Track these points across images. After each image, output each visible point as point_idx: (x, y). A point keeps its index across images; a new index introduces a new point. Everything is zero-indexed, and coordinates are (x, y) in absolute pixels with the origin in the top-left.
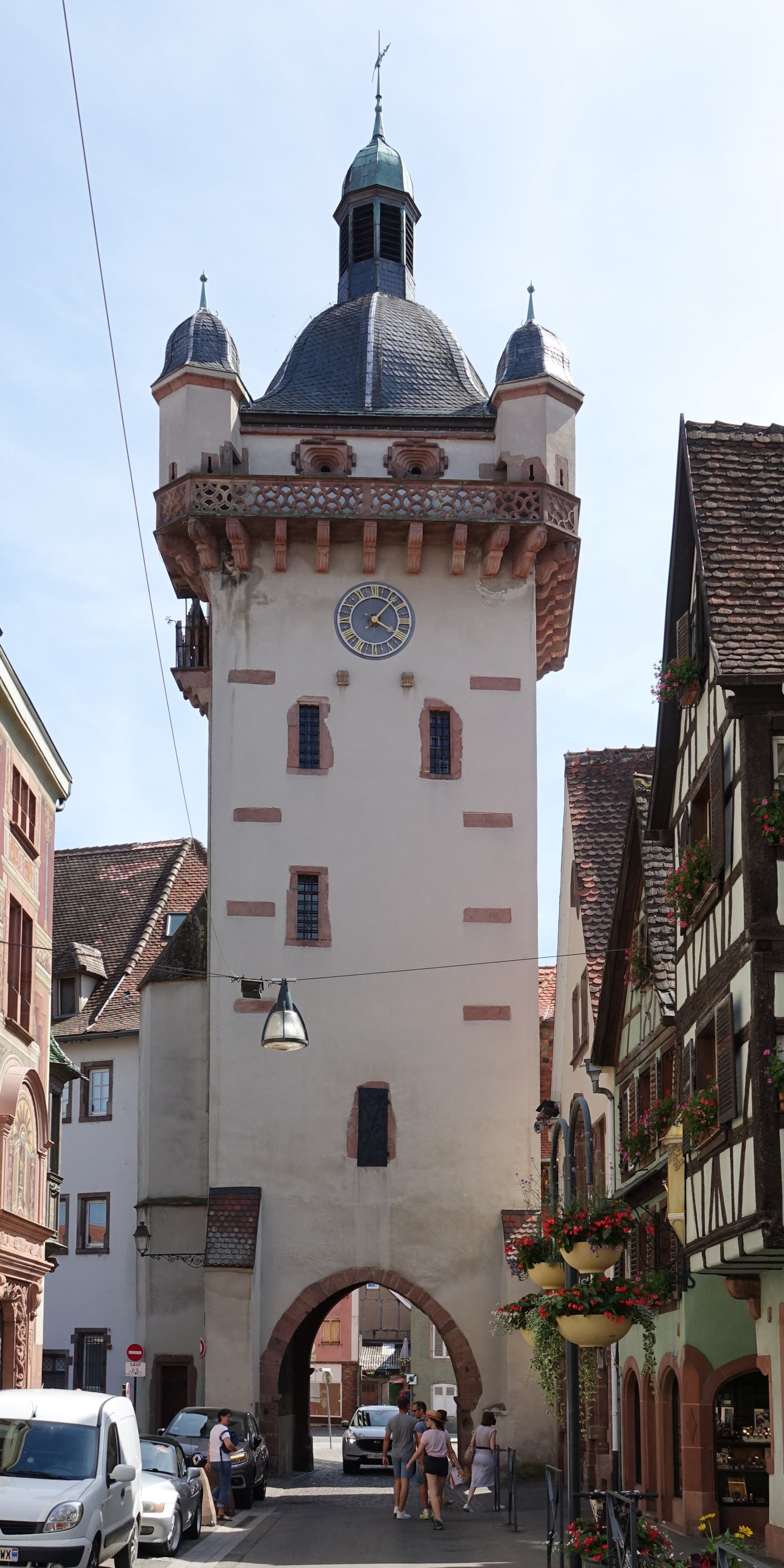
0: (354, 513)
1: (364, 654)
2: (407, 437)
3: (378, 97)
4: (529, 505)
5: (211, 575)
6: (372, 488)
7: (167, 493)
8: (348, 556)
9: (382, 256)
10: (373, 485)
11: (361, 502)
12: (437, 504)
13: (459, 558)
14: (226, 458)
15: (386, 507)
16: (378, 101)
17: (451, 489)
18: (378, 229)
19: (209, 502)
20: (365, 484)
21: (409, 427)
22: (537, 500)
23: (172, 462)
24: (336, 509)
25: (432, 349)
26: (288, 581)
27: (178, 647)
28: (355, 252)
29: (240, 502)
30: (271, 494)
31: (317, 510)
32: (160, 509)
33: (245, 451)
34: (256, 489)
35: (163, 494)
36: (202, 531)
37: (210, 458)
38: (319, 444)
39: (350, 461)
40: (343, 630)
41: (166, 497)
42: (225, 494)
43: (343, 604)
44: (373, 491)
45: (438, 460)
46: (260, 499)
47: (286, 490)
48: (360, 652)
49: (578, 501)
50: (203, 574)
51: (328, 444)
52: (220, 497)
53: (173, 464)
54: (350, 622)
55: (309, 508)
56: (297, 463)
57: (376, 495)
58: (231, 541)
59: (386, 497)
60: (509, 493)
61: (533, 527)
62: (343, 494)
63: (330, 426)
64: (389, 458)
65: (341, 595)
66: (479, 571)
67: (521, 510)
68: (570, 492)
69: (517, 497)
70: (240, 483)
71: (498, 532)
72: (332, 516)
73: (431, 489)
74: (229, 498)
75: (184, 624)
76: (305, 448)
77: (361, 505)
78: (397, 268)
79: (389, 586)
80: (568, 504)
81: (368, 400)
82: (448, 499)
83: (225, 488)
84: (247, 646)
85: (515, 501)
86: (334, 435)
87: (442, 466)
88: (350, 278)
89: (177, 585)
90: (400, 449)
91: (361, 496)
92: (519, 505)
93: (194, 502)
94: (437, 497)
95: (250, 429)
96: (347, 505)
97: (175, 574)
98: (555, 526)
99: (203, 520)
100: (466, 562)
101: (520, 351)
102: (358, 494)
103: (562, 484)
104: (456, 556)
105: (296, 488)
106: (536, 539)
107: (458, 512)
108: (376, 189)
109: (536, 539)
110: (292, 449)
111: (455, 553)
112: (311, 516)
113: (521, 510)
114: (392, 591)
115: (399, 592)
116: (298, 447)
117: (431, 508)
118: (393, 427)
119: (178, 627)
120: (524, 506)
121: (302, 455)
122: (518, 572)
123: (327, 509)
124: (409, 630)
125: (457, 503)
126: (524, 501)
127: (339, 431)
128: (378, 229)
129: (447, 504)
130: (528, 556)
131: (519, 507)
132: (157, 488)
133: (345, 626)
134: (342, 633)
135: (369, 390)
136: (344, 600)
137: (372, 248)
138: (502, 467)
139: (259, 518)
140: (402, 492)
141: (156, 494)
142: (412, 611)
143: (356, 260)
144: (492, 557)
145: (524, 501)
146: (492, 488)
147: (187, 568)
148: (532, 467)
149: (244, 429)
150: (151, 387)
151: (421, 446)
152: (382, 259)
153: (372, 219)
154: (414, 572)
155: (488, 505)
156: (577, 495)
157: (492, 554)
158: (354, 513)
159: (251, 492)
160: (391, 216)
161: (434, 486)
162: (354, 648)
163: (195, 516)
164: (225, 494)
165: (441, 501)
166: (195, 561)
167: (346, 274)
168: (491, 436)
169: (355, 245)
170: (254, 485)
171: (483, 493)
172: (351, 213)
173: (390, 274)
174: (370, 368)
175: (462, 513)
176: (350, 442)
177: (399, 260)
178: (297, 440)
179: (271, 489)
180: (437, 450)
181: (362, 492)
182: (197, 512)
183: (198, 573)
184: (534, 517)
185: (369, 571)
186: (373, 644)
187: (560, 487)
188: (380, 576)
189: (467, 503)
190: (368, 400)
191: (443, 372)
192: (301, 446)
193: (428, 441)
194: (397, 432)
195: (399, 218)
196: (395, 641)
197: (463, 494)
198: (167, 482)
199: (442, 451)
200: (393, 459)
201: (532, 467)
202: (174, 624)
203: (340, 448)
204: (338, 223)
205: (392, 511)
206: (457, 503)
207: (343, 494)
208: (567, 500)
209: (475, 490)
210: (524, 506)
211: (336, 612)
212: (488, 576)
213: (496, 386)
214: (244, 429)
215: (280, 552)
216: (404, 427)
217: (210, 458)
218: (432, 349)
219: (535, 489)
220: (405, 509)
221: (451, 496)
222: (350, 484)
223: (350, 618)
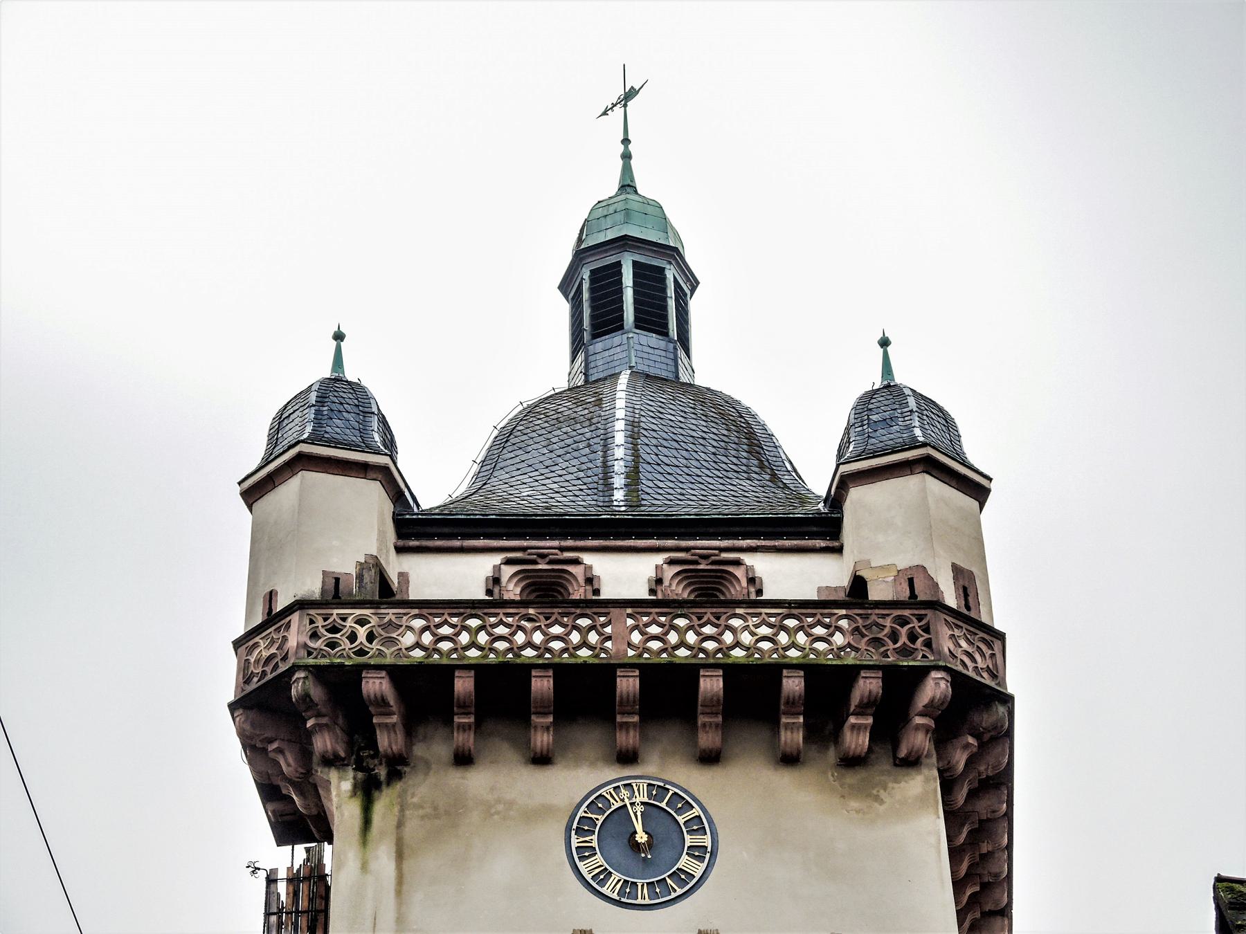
0: (597, 656)
1: (623, 900)
2: (687, 550)
3: (626, 141)
4: (913, 637)
5: (333, 775)
6: (629, 616)
7: (257, 639)
8: (589, 737)
9: (637, 327)
10: (629, 611)
11: (609, 638)
12: (746, 638)
13: (792, 736)
14: (367, 578)
15: (655, 645)
16: (626, 147)
17: (770, 615)
18: (629, 295)
19: (332, 645)
20: (615, 612)
21: (692, 536)
22: (926, 629)
23: (269, 590)
24: (565, 650)
25: (725, 432)
26: (477, 781)
27: (268, 914)
28: (594, 326)
29: (391, 641)
30: (446, 630)
31: (529, 652)
32: (244, 668)
33: (403, 576)
34: (418, 623)
35: (251, 643)
36: (317, 693)
37: (337, 580)
38: (535, 562)
39: (589, 588)
40: (582, 858)
41: (256, 645)
42: (362, 632)
43: (581, 813)
44: (630, 622)
45: (744, 583)
46: (427, 638)
47: (474, 623)
48: (615, 896)
49: (1001, 637)
50: (320, 773)
51: (550, 562)
52: (353, 637)
53: (271, 593)
54: (595, 844)
55: (516, 650)
56: (496, 590)
57: (636, 627)
58: (372, 709)
59: (654, 630)
60: (874, 617)
61: (921, 673)
62: (576, 627)
63: (553, 536)
64: (659, 581)
65: (578, 800)
66: (832, 755)
67: (898, 645)
68: (985, 619)
69: (888, 622)
70: (390, 614)
71: (861, 682)
72: (557, 660)
73: (735, 616)
74: (371, 637)
75: (282, 874)
76: (508, 571)
77: (608, 644)
78: (662, 344)
79: (666, 782)
80: (983, 640)
81: (619, 495)
82: (764, 631)
83: (362, 622)
84: (399, 892)
85: (886, 631)
86: (562, 549)
87: (752, 590)
88: (586, 360)
89: (274, 812)
90: (678, 568)
91: (608, 630)
92: (894, 636)
93: (306, 645)
94: (746, 628)
95: (414, 543)
96: (584, 644)
97: (269, 791)
98: (965, 672)
99: (319, 673)
100: (806, 739)
101: (874, 418)
102: (604, 625)
103: (968, 608)
104: (787, 726)
105: (492, 620)
106: (935, 688)
107: (786, 649)
108: (624, 243)
109: (935, 688)
110: (489, 572)
111: (784, 720)
112: (518, 661)
113: (898, 645)
114: (673, 789)
115: (685, 791)
116: (497, 569)
117: (737, 644)
118: (661, 536)
119: (271, 880)
120: (903, 639)
121: (504, 579)
122: (903, 753)
123: (549, 650)
124: (708, 856)
125: (783, 638)
126: (904, 631)
127: (570, 543)
128: (629, 295)
129: (764, 638)
130: (918, 739)
131: (895, 642)
132: (240, 631)
133: (585, 852)
134: (580, 865)
135: (619, 481)
136: (584, 807)
137: (621, 318)
138: (858, 585)
139: (420, 668)
140: (681, 622)
141: (237, 644)
142: (711, 822)
143: (595, 336)
144: (853, 726)
145: (904, 631)
146: (843, 612)
147: (288, 764)
148: (911, 582)
149: (401, 543)
150: (239, 483)
151: (714, 563)
152: (638, 331)
153: (620, 282)
154: (710, 758)
155: (839, 639)
156: (998, 626)
157: (852, 720)
158: (597, 656)
159: (410, 628)
160: (649, 279)
161: (739, 611)
162: (604, 890)
163: (306, 667)
164: (362, 632)
165: (753, 634)
166: (305, 753)
167: (581, 358)
168: (836, 544)
169: (592, 317)
170: (416, 617)
171: (828, 620)
172: (586, 275)
173: (651, 351)
174: (619, 453)
175: (793, 653)
176: (587, 558)
177: (663, 331)
178: (497, 559)
179: (446, 622)
180: (743, 568)
181: (609, 623)
182: (311, 661)
183: (309, 772)
184: (924, 656)
185: (627, 758)
186: (639, 882)
187: (965, 611)
188: (651, 767)
189: (801, 638)
190: (619, 495)
191: (744, 461)
192: (502, 566)
193: (725, 555)
194: (670, 543)
195: (663, 279)
196: (681, 876)
197: (791, 623)
198: (258, 619)
199: (749, 569)
200: (666, 583)
201: (911, 582)
202: (262, 875)
203: (570, 568)
204: (567, 297)
205: (664, 650)
206: (783, 638)
207: (576, 627)
208: (982, 635)
209: (813, 615)
210: (903, 639)
211: (568, 829)
212: (851, 762)
213: (838, 466)
214: (401, 543)
215: (464, 728)
216: (682, 536)
217: (337, 580)
218: (725, 432)
219: (923, 612)
220: (689, 647)
221: (771, 626)
222: (588, 611)
223: (595, 837)
